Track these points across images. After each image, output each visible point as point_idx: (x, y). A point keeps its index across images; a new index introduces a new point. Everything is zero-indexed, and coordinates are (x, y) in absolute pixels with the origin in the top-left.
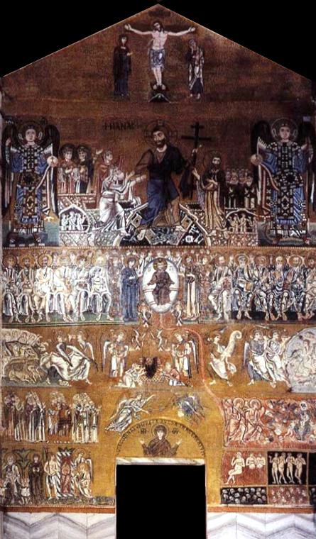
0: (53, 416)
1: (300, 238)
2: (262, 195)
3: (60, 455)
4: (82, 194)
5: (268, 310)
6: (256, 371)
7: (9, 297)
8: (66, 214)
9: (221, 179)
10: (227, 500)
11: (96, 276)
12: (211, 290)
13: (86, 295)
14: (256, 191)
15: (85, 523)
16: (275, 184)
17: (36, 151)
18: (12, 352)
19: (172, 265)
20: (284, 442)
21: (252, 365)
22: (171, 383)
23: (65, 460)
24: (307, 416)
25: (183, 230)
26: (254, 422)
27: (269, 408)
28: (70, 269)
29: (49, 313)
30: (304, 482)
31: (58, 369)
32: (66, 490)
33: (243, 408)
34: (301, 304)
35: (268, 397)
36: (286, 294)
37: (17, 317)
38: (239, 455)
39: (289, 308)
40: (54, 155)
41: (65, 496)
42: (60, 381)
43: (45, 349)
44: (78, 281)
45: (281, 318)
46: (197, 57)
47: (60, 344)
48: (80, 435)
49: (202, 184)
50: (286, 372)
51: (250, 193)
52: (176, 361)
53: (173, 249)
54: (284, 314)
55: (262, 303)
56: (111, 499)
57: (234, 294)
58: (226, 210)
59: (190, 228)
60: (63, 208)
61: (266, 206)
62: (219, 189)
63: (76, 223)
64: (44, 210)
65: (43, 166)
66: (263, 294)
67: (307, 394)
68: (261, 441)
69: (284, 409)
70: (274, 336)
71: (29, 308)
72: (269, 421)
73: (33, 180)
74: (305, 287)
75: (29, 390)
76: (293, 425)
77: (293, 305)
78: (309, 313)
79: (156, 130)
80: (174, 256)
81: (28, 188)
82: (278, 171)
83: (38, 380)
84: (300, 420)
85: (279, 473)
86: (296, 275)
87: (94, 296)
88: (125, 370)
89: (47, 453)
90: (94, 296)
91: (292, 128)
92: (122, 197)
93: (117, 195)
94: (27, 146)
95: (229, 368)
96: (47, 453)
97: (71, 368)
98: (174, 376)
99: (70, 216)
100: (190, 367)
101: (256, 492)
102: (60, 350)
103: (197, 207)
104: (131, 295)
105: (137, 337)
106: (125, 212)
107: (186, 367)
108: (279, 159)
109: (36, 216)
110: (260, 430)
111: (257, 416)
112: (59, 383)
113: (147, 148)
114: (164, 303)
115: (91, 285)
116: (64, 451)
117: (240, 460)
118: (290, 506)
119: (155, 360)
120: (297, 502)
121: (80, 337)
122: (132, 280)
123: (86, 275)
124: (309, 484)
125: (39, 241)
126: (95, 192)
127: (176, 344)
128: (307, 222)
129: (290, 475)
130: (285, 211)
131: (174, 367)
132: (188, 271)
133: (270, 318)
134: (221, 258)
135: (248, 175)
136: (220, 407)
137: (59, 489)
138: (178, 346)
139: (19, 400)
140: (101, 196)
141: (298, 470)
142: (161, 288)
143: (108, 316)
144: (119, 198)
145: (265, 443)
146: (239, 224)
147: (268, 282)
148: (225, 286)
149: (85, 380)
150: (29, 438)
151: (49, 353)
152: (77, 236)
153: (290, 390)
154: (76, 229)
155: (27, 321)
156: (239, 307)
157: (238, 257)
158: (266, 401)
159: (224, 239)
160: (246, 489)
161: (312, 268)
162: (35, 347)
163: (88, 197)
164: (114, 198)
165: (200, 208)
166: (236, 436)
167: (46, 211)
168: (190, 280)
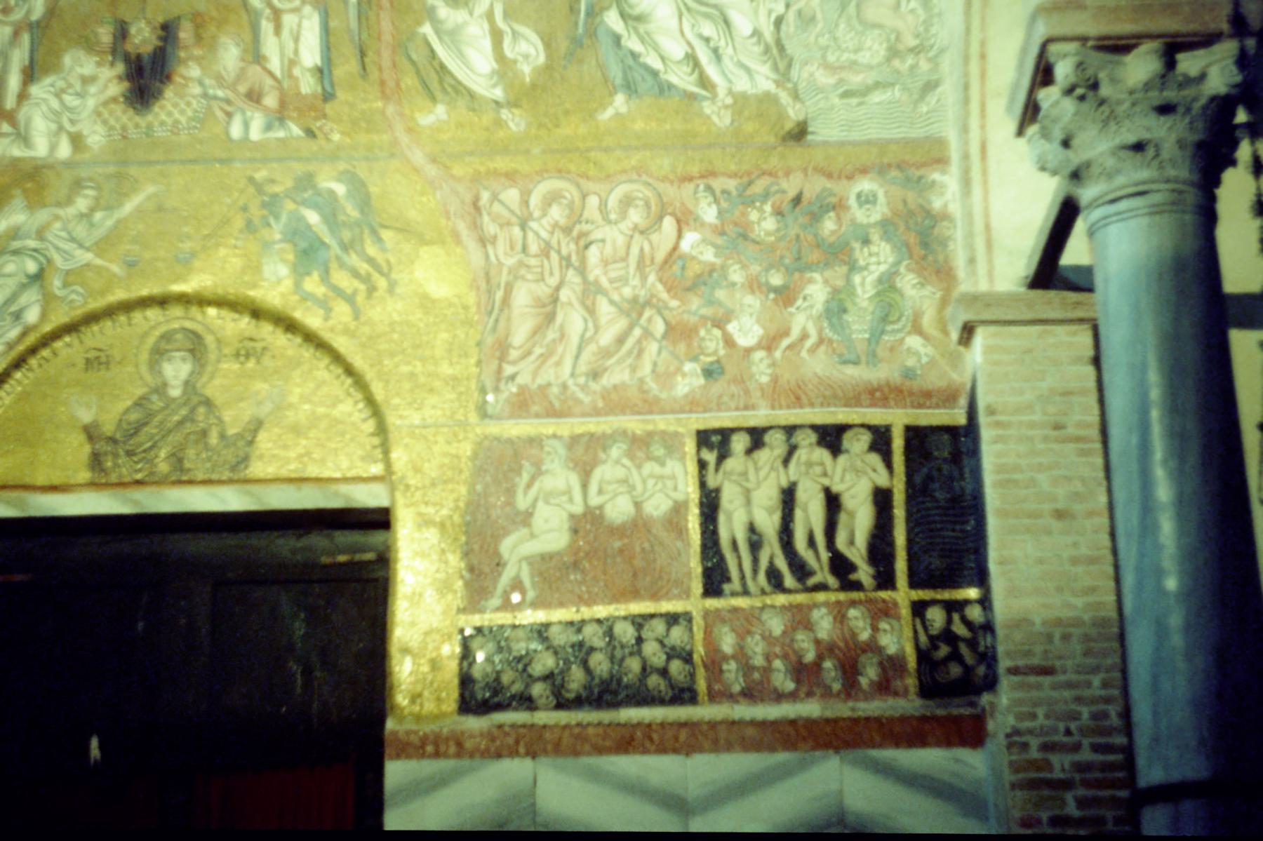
6: (635, 56)
20: (775, 380)
22: (236, 131)
26: (627, 292)
27: (699, 223)
30: (885, 580)
52: (266, 26)
67: (883, 145)
68: (665, 377)
69: (770, 224)
72: (706, 279)
76: (817, 291)
84: (853, 267)
95: (508, 52)
98: (254, 97)
100: (327, 48)
101: (640, 640)
107: (311, 55)
110: (659, 327)
111: (641, 265)
117: (560, 477)
120: (850, 687)
129: (811, 542)
131: (255, 56)
136: (462, 227)
141: (852, 515)
153: (799, 133)
158: (690, 187)
160: (589, 630)
166: (544, 358)
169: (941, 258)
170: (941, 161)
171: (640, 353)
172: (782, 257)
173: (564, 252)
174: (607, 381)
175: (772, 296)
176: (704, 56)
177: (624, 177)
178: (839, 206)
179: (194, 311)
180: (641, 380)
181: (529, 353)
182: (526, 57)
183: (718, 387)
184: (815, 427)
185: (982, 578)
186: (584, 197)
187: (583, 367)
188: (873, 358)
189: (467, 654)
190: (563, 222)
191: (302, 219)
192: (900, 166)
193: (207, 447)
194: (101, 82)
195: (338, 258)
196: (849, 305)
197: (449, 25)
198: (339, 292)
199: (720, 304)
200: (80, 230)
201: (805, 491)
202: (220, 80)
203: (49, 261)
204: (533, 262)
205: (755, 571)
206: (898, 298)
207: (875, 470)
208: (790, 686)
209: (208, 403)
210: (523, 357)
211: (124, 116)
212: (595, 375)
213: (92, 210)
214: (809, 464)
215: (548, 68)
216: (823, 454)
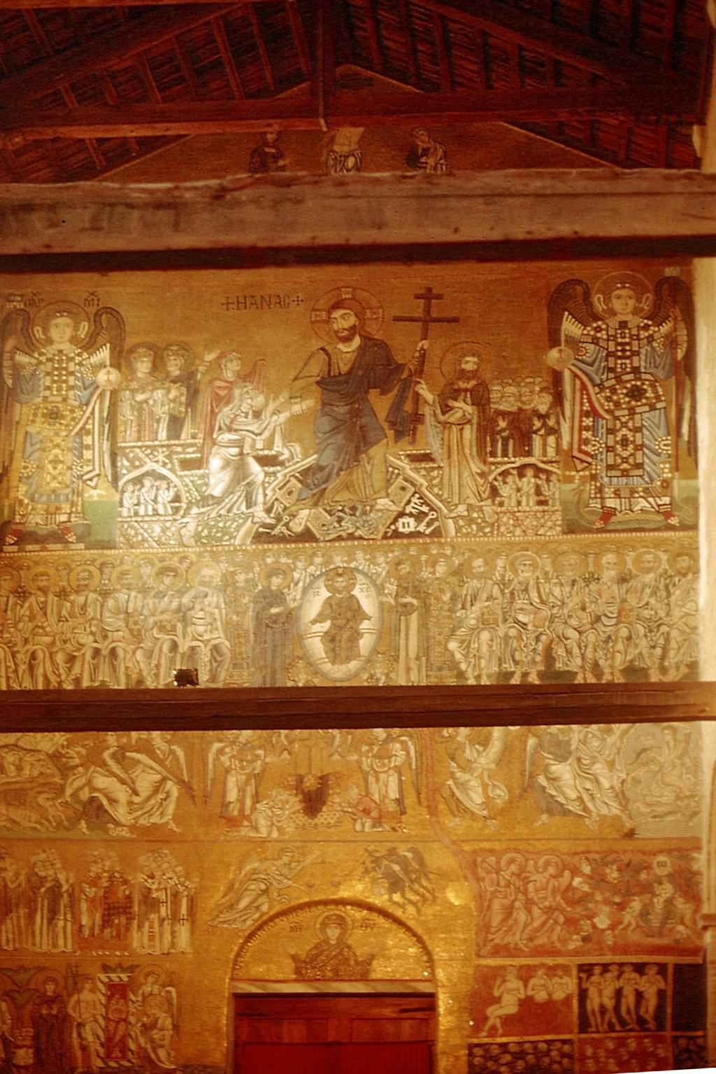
0: (92, 901)
1: (658, 512)
2: (572, 428)
4: (173, 442)
5: (582, 667)
6: (552, 796)
8: (135, 484)
9: (480, 399)
11: (198, 607)
12: (453, 630)
13: (174, 646)
14: (558, 423)
16: (602, 406)
17: (72, 359)
19: (367, 581)
20: (615, 943)
22: (358, 827)
23: (118, 991)
25: (394, 508)
26: (547, 904)
27: (582, 875)
28: (140, 596)
30: (660, 1027)
31: (105, 802)
32: (117, 1053)
33: (521, 874)
34: (658, 651)
35: (580, 849)
36: (624, 632)
39: (631, 661)
40: (111, 365)
41: (113, 1064)
42: (111, 826)
43: (77, 761)
44: (156, 619)
46: (431, 161)
47: (112, 750)
48: (152, 938)
49: (438, 411)
50: (622, 797)
51: (544, 425)
52: (371, 779)
53: (371, 550)
55: (569, 652)
57: (507, 637)
58: (493, 464)
59: (409, 502)
60: (129, 472)
61: (580, 451)
62: (475, 421)
63: (155, 501)
64: (85, 478)
65: (85, 389)
66: (571, 633)
68: (564, 941)
69: (615, 875)
71: (45, 676)
73: (63, 417)
74: (668, 615)
75: (38, 842)
76: (636, 905)
77: (640, 654)
78: (678, 669)
79: (337, 305)
80: (373, 561)
81: (52, 433)
82: (608, 379)
83: (59, 824)
84: (654, 895)
85: (603, 1010)
86: (648, 591)
88: (257, 798)
90: (193, 649)
91: (639, 289)
92: (259, 445)
93: (248, 442)
94: (50, 351)
96: (75, 976)
97: (136, 799)
98: (366, 812)
99: (143, 486)
100: (401, 791)
101: (549, 1050)
102: (111, 763)
103: (427, 458)
106: (267, 474)
107: (393, 794)
108: (608, 355)
109: (68, 491)
110: (562, 919)
112: (106, 831)
113: (315, 344)
114: (348, 659)
115: (185, 627)
116: (114, 971)
117: (514, 983)
119: (323, 779)
122: (277, 615)
123: (174, 605)
124: (675, 1028)
125: (72, 539)
126: (201, 435)
127: (371, 744)
128: (672, 478)
129: (629, 1012)
130: (625, 460)
132: (403, 590)
134: (478, 563)
135: (542, 390)
137: (102, 1051)
138: (376, 749)
140: (214, 444)
141: (648, 1001)
142: (341, 628)
144: (253, 447)
145: (572, 946)
146: (519, 490)
147: (583, 609)
148: (485, 622)
149: (167, 823)
150: (34, 944)
151: (87, 769)
152: (157, 529)
154: (156, 513)
156: (516, 663)
157: (516, 558)
158: (576, 859)
159: (484, 521)
161: (685, 575)
163: (184, 446)
164: (242, 447)
165: (433, 460)
166: (507, 932)
167: (91, 480)
168: (406, 609)
171: (552, 931)
176: (586, 797)
178: (649, 867)
179: (341, 907)
180: (553, 942)
181: (500, 930)
182: (499, 796)
183: (589, 946)
184: (632, 964)
185: (704, 1028)
186: (527, 860)
187: (525, 936)
188: (661, 935)
189: (470, 1055)
190: (517, 872)
191: (391, 868)
192: (678, 850)
193: (349, 966)
197: (461, 780)
198: (410, 902)
199: (591, 910)
200: (285, 871)
202: (350, 805)
203: (271, 884)
205: (603, 1022)
208: (617, 1069)
209: (349, 947)
210: (497, 931)
212: (531, 939)
213: (291, 862)
214: (629, 979)
215: (510, 802)
216: (634, 975)
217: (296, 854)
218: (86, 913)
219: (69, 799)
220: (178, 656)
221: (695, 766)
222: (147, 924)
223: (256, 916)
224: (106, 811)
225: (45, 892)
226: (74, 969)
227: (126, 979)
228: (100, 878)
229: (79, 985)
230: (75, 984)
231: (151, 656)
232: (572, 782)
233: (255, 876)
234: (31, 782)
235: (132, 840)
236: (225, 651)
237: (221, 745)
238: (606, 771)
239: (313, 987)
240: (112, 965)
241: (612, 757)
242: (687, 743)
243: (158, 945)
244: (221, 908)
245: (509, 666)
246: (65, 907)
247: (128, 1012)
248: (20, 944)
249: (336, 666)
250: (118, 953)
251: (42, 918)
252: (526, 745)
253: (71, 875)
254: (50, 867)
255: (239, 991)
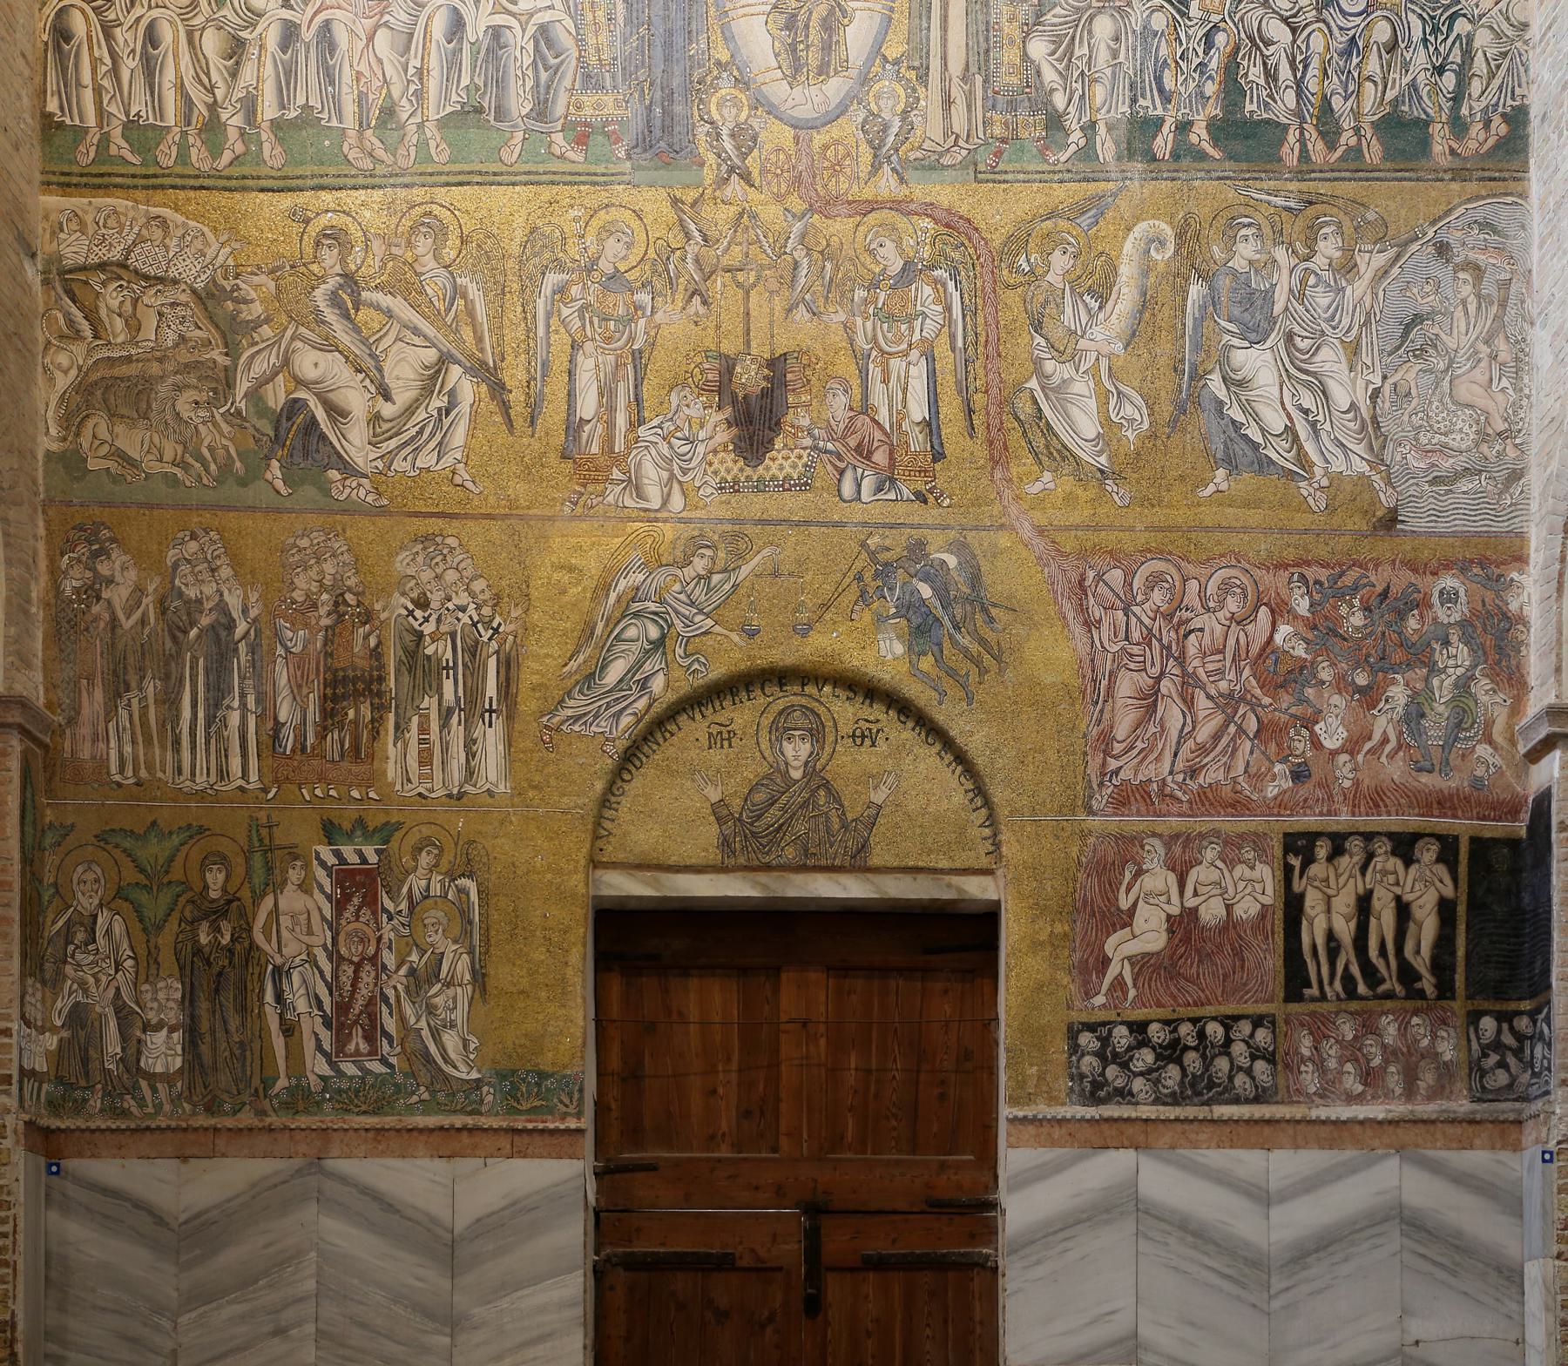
0: (298, 662)
3: (331, 860)
7: (78, 24)
10: (1097, 1085)
15: (444, 1215)
18: (91, 316)
21: (1222, 393)
24: (1463, 651)
26: (1223, 685)
29: (276, 125)
34: (1449, 80)
35: (1290, 555)
37: (117, 134)
38: (1154, 855)
43: (257, 309)
45: (1355, 152)
47: (332, 283)
48: (425, 759)
50: (1372, 428)
54: (1368, 132)
56: (571, 1086)
67: (1466, 538)
68: (1256, 778)
70: (1321, 244)
71: (180, 87)
76: (1398, 694)
83: (226, 468)
87: (496, 32)
89: (268, 850)
102: (330, 315)
104: (670, 33)
105: (692, 249)
110: (1252, 725)
112: (326, 492)
116: (349, 837)
118: (1376, 1111)
121: (423, 245)
133: (1304, 155)
139: (132, 574)
143: (558, 138)
150: (180, 773)
153: (1390, 521)
155: (167, 156)
162: (209, 298)
169: (1514, 662)
170: (1520, 559)
171: (1235, 750)
172: (1368, 655)
173: (1165, 641)
174: (1204, 779)
175: (1357, 696)
177: (1223, 563)
178: (1423, 604)
181: (1132, 748)
192: (1483, 563)
194: (709, 426)
195: (951, 637)
196: (1427, 710)
198: (952, 673)
200: (699, 594)
201: (1379, 899)
204: (1136, 650)
206: (1472, 704)
207: (1441, 881)
211: (730, 466)
215: (1153, 436)
217: (721, 554)
218: (286, 692)
219: (243, 405)
220: (466, 47)
221: (1517, 359)
222: (415, 719)
223: (641, 704)
224: (323, 437)
225: (199, 637)
226: (264, 832)
227: (373, 858)
228: (315, 606)
229: (277, 872)
230: (269, 869)
231: (408, 48)
232: (1275, 391)
233: (636, 607)
234: (160, 360)
235: (382, 511)
236: (566, 41)
237: (565, 277)
238: (1344, 366)
239: (756, 884)
240: (347, 826)
241: (1354, 332)
242: (1503, 305)
243: (438, 775)
244: (570, 683)
245: (1151, 105)
246: (242, 678)
247: (379, 939)
248: (150, 767)
249: (798, 90)
250: (355, 794)
251: (194, 706)
252: (1185, 299)
253: (254, 597)
254: (206, 576)
255: (606, 892)
